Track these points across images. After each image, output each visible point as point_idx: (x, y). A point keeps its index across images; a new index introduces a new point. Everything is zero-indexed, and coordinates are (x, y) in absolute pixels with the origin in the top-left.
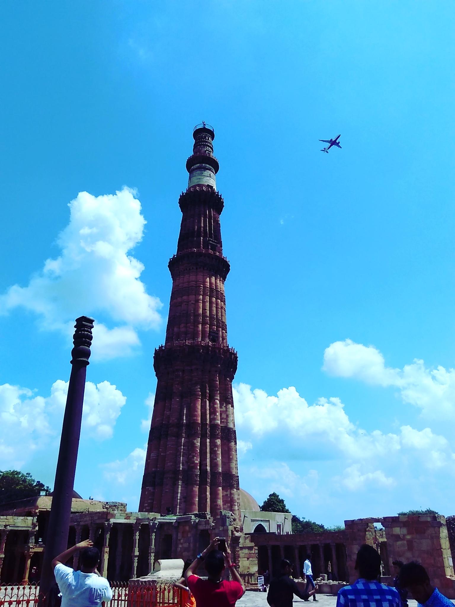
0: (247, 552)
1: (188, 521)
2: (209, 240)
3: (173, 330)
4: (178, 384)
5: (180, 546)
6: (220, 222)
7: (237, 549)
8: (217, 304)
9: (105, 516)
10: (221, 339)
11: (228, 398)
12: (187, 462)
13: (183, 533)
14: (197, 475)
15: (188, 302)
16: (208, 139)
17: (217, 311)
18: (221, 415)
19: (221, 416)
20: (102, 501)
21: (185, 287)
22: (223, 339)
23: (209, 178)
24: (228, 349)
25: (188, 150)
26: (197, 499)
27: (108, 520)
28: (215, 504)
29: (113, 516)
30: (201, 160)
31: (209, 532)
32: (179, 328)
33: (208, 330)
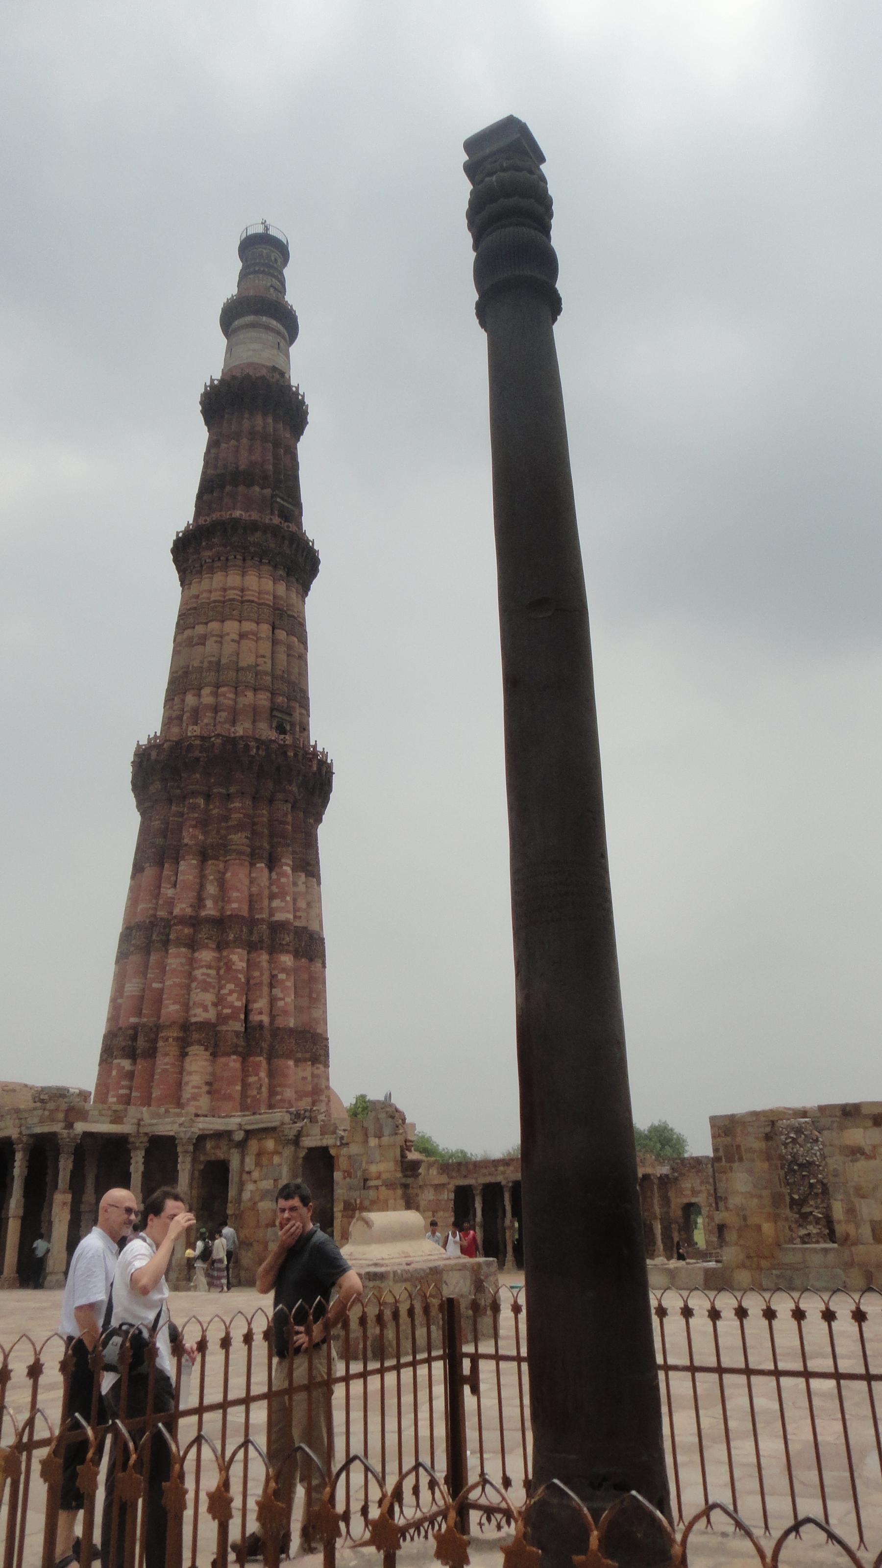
0: (431, 1197)
1: (274, 1129)
2: (273, 496)
3: (183, 701)
4: (195, 827)
5: (250, 1187)
6: (300, 459)
7: (415, 1191)
8: (289, 647)
9: (61, 1116)
10: (297, 729)
11: (308, 864)
12: (215, 1005)
13: (259, 1154)
14: (237, 1034)
15: (221, 637)
16: (276, 260)
17: (289, 662)
18: (295, 900)
19: (294, 904)
20: (30, 1082)
21: (215, 601)
22: (305, 728)
23: (275, 351)
24: (315, 754)
25: (225, 281)
26: (239, 1088)
27: (70, 1126)
28: (279, 1097)
29: (83, 1115)
30: (260, 305)
31: (333, 1152)
32: (199, 696)
33: (267, 704)
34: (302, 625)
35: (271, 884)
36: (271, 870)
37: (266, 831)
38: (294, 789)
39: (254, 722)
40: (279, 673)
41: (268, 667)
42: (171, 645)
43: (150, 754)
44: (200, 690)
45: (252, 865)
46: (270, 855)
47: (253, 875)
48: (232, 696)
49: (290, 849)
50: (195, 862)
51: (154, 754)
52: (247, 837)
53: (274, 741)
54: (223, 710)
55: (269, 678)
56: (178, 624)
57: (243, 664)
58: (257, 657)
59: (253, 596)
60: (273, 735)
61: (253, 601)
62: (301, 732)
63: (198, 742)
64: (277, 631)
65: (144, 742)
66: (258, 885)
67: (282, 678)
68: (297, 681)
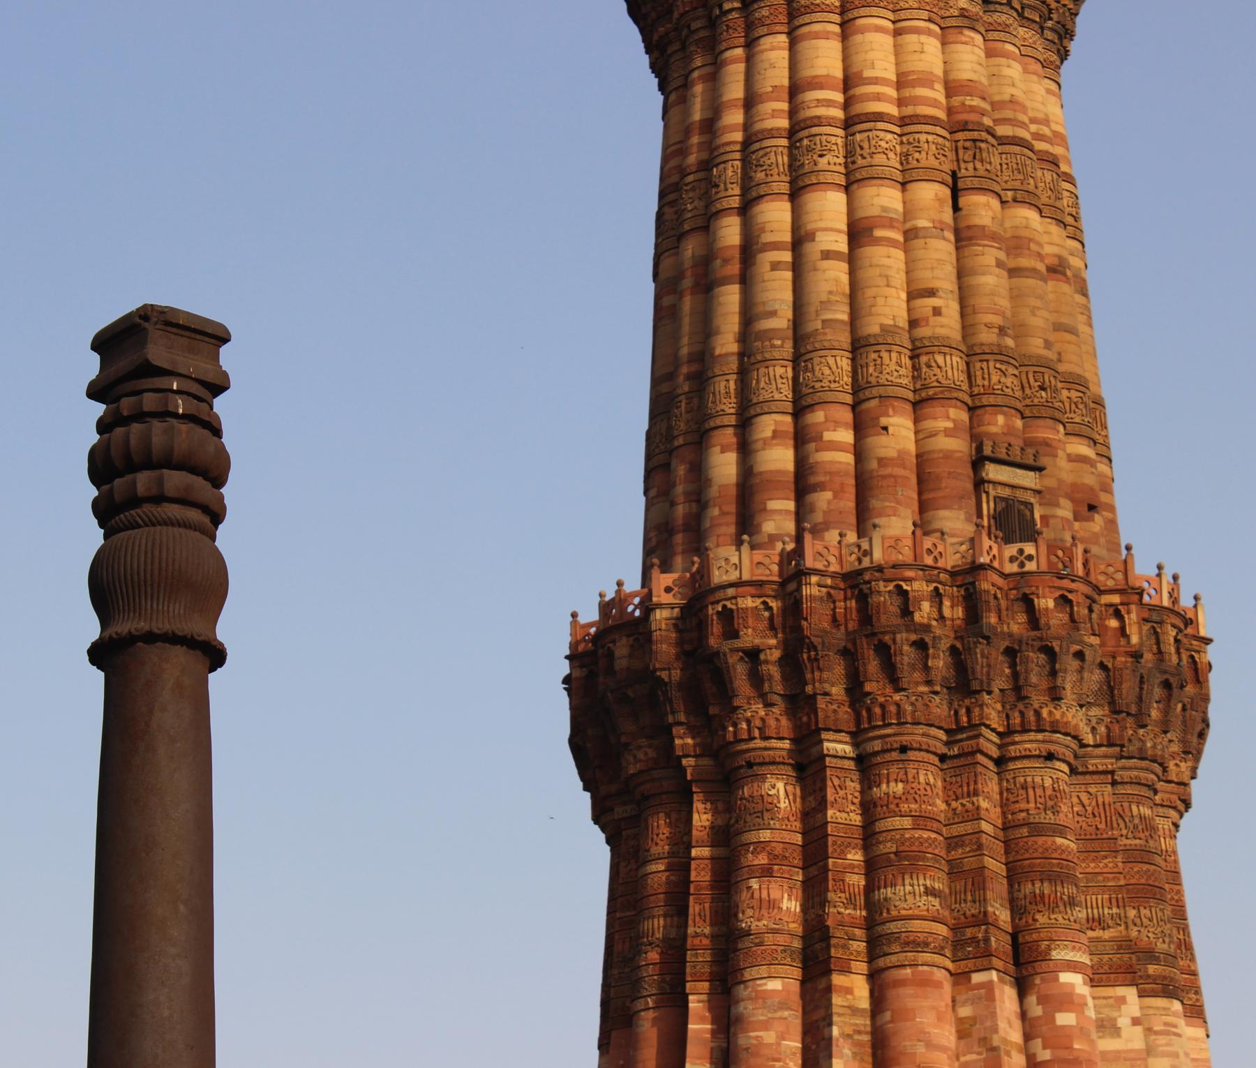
3: (699, 470)
4: (767, 872)
8: (1016, 244)
10: (1065, 511)
11: (1150, 955)
17: (1016, 296)
32: (745, 449)
33: (959, 446)
34: (1052, 162)
35: (1028, 1037)
36: (1022, 987)
37: (995, 865)
38: (1075, 717)
39: (923, 507)
40: (987, 337)
41: (948, 324)
42: (650, 287)
43: (610, 655)
44: (744, 423)
45: (960, 978)
46: (1014, 937)
47: (965, 1011)
48: (846, 436)
49: (1080, 914)
50: (774, 985)
51: (621, 649)
52: (929, 892)
53: (982, 567)
54: (820, 487)
55: (957, 360)
56: (659, 216)
57: (872, 327)
58: (912, 296)
59: (878, 97)
60: (989, 550)
61: (879, 117)
62: (1077, 518)
63: (749, 603)
64: (962, 201)
65: (590, 614)
66: (984, 1041)
67: (1000, 354)
68: (1051, 355)
